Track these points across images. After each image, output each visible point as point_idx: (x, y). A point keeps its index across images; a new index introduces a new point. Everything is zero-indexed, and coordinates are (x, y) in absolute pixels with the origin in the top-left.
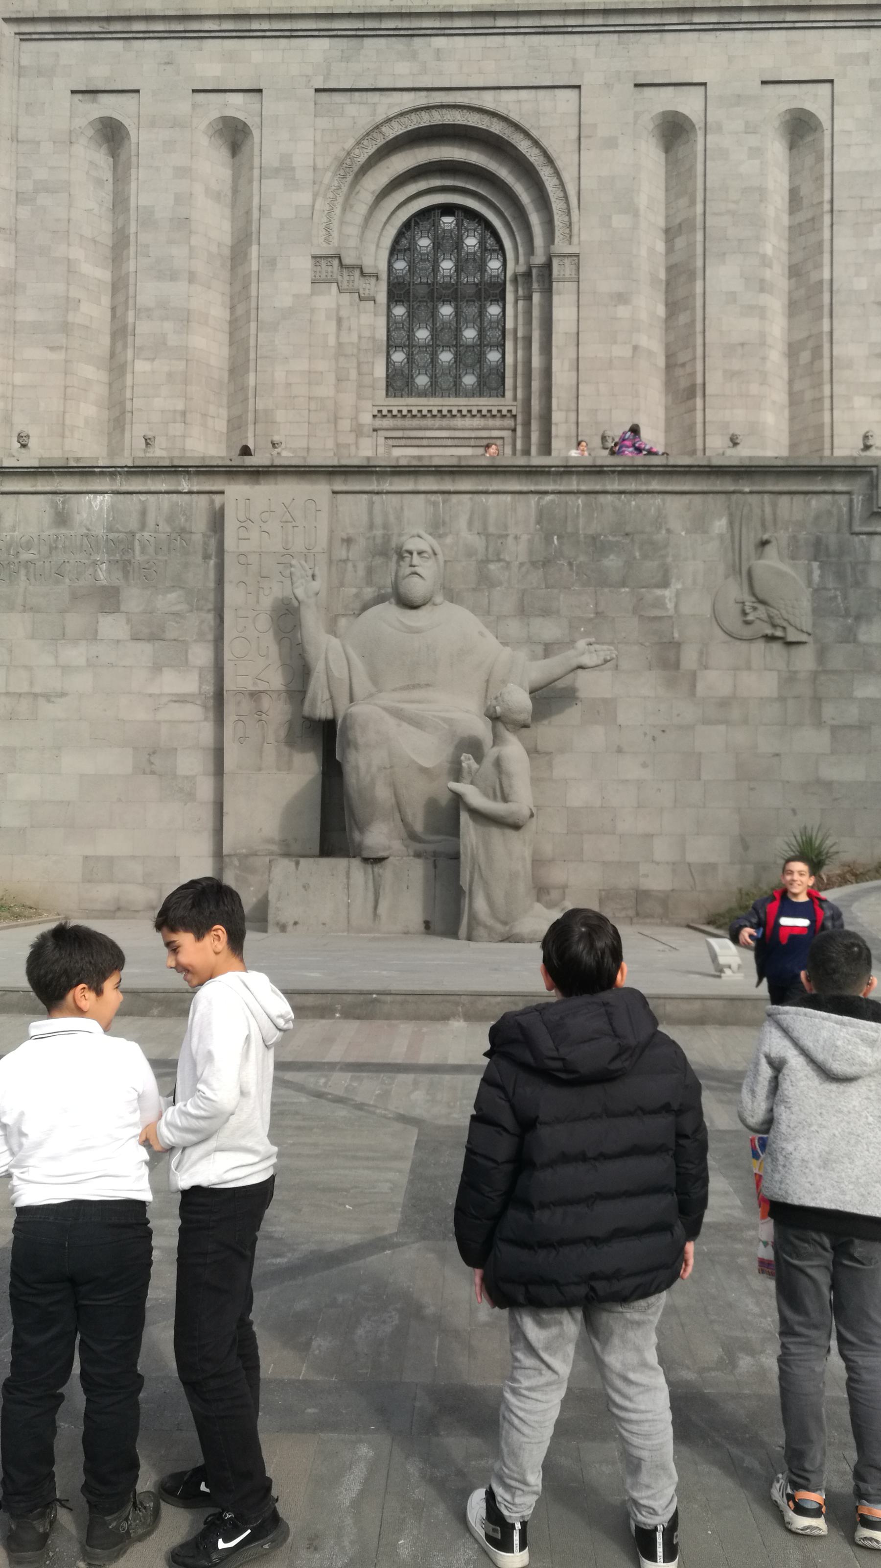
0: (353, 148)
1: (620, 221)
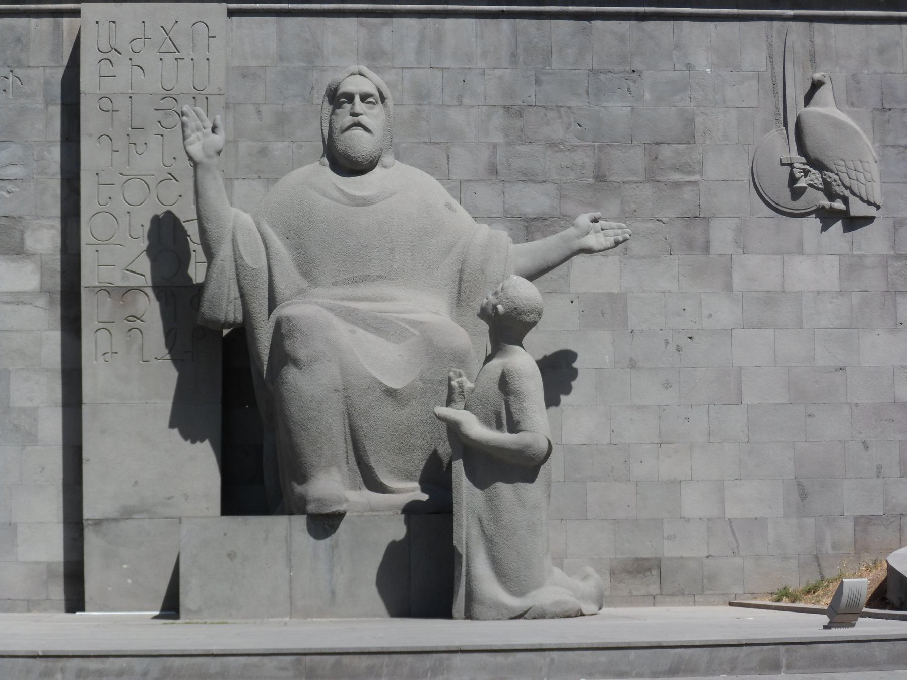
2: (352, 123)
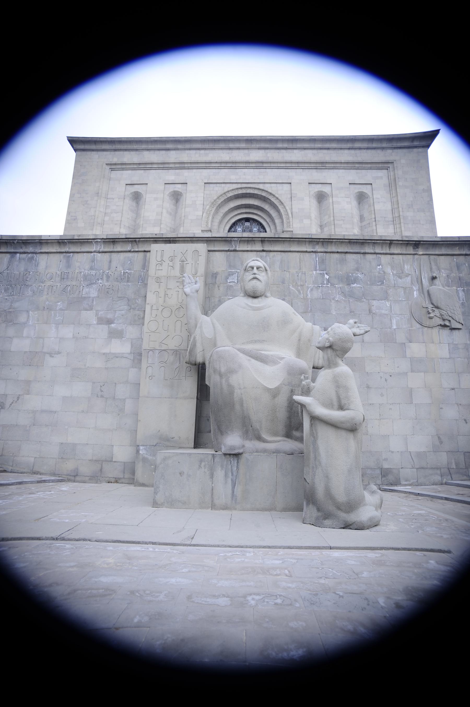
0: (217, 199)
1: (306, 222)
2: (252, 277)
